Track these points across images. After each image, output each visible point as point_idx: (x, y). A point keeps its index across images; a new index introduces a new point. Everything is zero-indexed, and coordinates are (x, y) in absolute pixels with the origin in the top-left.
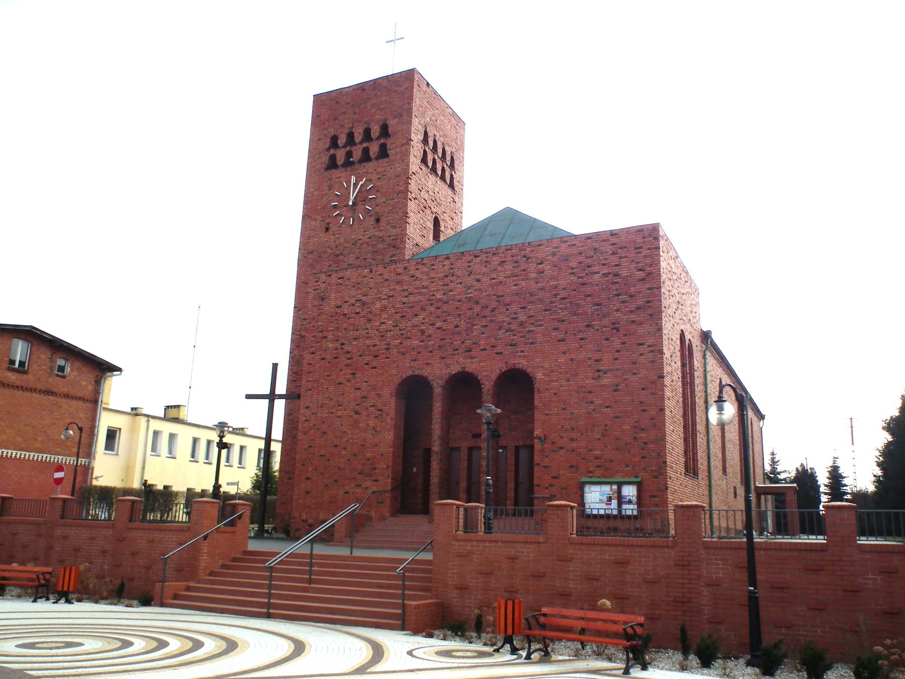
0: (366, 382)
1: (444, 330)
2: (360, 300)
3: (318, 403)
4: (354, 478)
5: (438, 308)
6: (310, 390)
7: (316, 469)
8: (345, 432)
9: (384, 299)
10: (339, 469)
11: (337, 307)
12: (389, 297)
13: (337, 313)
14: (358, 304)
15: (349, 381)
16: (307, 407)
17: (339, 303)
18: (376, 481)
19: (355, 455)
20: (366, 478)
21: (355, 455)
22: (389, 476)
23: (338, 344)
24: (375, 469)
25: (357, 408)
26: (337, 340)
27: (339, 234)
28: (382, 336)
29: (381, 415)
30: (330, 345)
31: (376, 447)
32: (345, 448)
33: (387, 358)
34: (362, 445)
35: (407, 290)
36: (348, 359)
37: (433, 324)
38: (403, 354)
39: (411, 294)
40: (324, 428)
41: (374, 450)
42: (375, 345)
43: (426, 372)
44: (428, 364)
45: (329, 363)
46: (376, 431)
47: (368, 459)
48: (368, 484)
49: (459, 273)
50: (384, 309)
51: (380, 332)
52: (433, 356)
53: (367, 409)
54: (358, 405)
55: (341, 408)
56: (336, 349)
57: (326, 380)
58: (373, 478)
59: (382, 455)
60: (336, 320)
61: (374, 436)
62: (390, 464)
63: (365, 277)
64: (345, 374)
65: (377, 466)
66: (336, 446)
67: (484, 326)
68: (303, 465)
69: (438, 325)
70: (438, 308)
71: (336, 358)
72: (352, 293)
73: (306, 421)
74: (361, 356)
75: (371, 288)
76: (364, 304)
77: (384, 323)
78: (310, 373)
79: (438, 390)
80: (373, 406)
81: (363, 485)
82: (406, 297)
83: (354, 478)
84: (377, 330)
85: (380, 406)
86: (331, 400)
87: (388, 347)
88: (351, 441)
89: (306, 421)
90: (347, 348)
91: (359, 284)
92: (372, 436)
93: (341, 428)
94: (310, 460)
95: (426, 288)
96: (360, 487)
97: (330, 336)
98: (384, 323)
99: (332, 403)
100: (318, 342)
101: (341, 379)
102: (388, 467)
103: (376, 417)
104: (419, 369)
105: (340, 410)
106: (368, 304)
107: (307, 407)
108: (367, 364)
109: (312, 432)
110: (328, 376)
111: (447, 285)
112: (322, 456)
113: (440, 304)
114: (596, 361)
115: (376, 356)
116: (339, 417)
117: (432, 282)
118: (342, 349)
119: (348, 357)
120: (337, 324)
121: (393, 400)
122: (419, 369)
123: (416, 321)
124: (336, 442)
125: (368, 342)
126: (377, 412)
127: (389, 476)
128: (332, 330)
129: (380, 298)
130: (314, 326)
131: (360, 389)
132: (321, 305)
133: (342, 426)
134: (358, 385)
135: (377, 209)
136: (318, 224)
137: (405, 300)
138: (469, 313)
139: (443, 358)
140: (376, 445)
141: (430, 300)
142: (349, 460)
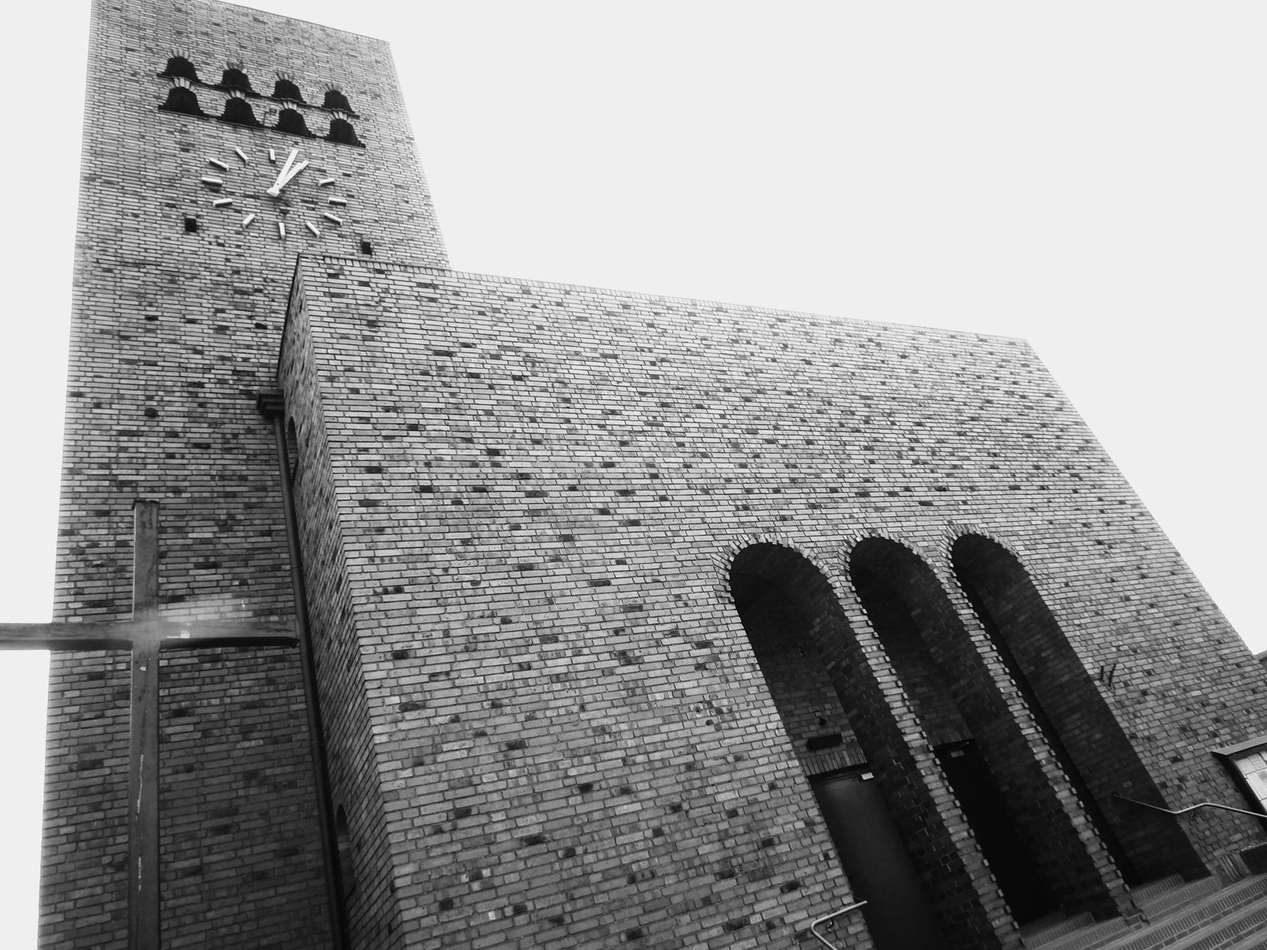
0: (619, 562)
1: (785, 446)
2: (516, 350)
3: (446, 634)
4: (707, 901)
5: (747, 400)
6: (399, 590)
7: (519, 910)
8: (603, 730)
9: (593, 359)
10: (632, 880)
11: (437, 353)
12: (605, 356)
13: (441, 368)
14: (509, 356)
15: (557, 559)
16: (400, 655)
17: (441, 344)
18: (792, 886)
19: (676, 808)
20: (752, 887)
21: (676, 808)
22: (827, 857)
23: (475, 452)
24: (768, 843)
25: (621, 643)
26: (469, 440)
27: (239, 247)
28: (623, 443)
29: (715, 658)
30: (444, 450)
31: (740, 765)
32: (626, 791)
33: (663, 498)
34: (690, 767)
35: (650, 350)
36: (530, 494)
37: (754, 432)
38: (706, 492)
39: (663, 360)
40: (507, 725)
41: (737, 775)
42: (611, 465)
43: (788, 537)
44: (783, 518)
45: (457, 502)
46: (719, 712)
47: (733, 814)
48: (769, 906)
49: (761, 342)
50: (600, 381)
51: (611, 433)
52: (788, 502)
53: (658, 644)
54: (617, 632)
55: (560, 646)
56: (475, 464)
57: (460, 556)
58: (778, 880)
59: (772, 787)
60: (445, 384)
61: (718, 729)
62: (814, 813)
63: (511, 299)
64: (536, 539)
65: (774, 831)
66: (586, 788)
67: (866, 448)
68: (446, 905)
69: (767, 434)
70: (747, 400)
71: (477, 489)
72: (484, 325)
73: (405, 708)
74: (573, 488)
75: (540, 328)
76: (529, 360)
77: (613, 412)
78: (380, 530)
79: (841, 585)
80: (674, 633)
81: (755, 919)
82: (653, 364)
83: (707, 901)
84: (602, 427)
85: (695, 630)
86: (505, 621)
87: (653, 471)
88: (640, 759)
89: (405, 708)
90: (513, 464)
91: (496, 310)
92: (712, 728)
93: (583, 716)
94: (477, 877)
95: (698, 354)
96: (747, 931)
97: (435, 424)
98: (613, 412)
99: (511, 632)
100: (388, 438)
101: (524, 554)
102: (810, 824)
103: (699, 667)
104: (768, 530)
105: (559, 655)
106: (544, 361)
107: (400, 655)
108: (604, 512)
109: (453, 751)
110: (465, 542)
111: (744, 357)
112: (534, 841)
113: (747, 393)
114: (1085, 525)
115: (624, 493)
116: (557, 678)
117: (708, 347)
118: (496, 465)
119: (529, 488)
120: (453, 395)
121: (732, 611)
122: (768, 530)
123: (702, 417)
124: (581, 771)
125: (584, 455)
126: (695, 652)
127: (827, 857)
128: (437, 411)
129: (577, 353)
130: (356, 391)
131: (607, 583)
132: (365, 338)
133: (583, 708)
134: (597, 572)
135: (358, 228)
136: (150, 208)
137: (654, 370)
138: (823, 420)
139: (813, 506)
140: (738, 759)
141: (719, 381)
142: (658, 832)
